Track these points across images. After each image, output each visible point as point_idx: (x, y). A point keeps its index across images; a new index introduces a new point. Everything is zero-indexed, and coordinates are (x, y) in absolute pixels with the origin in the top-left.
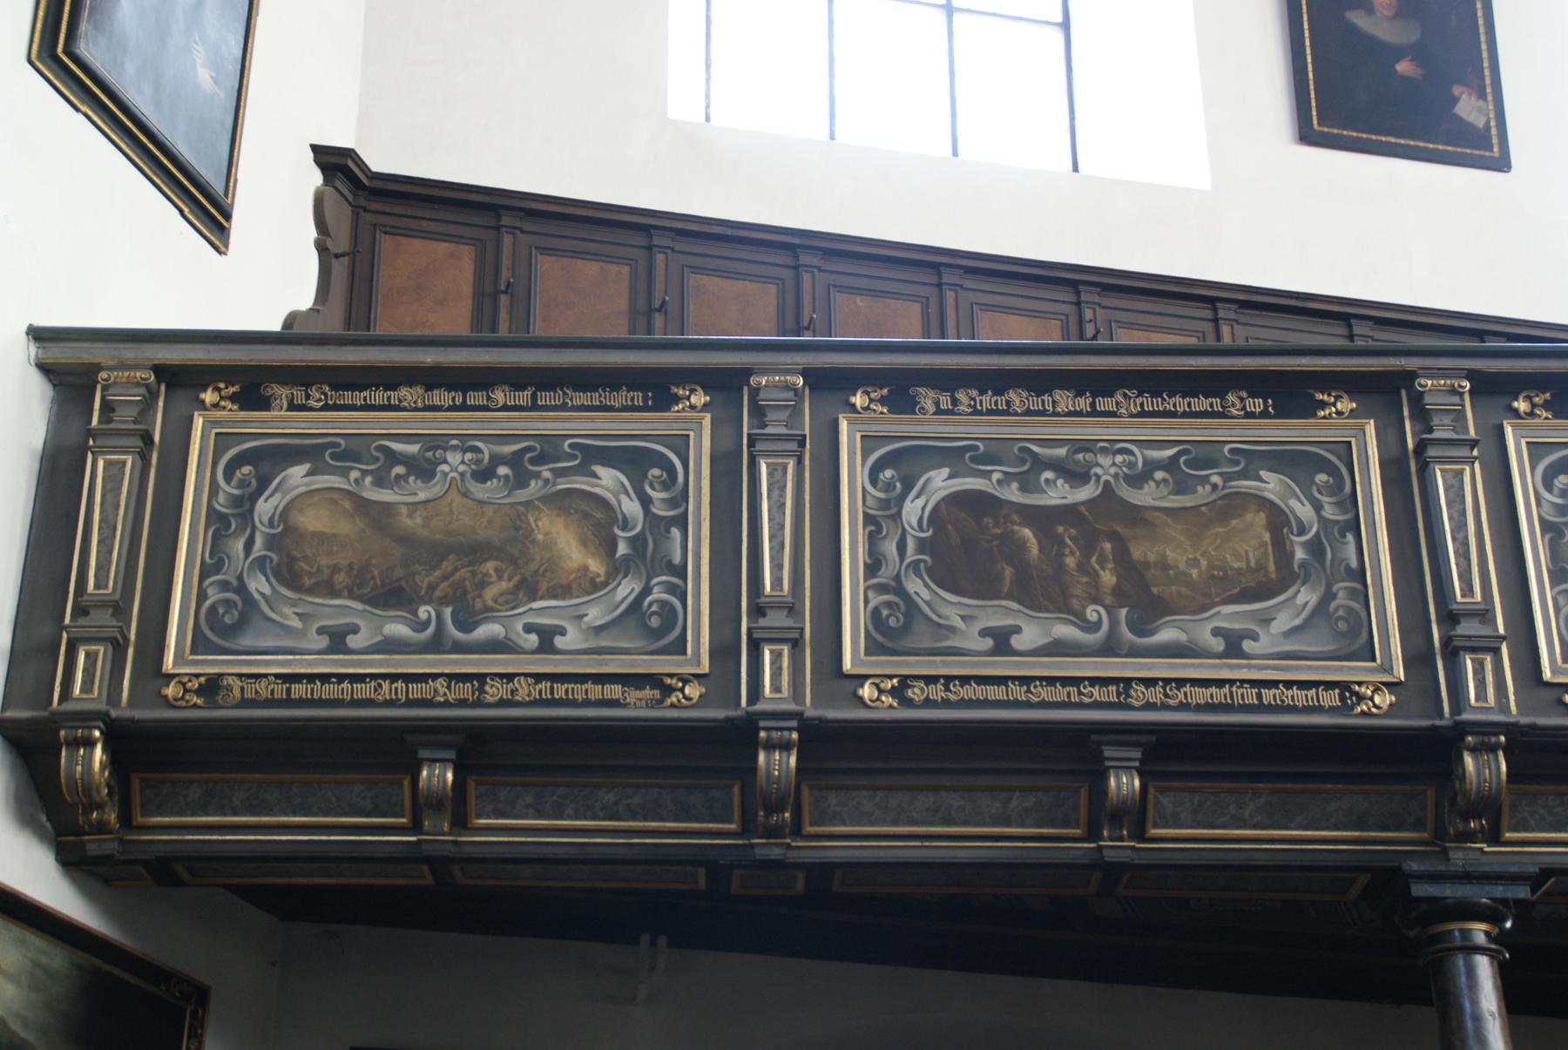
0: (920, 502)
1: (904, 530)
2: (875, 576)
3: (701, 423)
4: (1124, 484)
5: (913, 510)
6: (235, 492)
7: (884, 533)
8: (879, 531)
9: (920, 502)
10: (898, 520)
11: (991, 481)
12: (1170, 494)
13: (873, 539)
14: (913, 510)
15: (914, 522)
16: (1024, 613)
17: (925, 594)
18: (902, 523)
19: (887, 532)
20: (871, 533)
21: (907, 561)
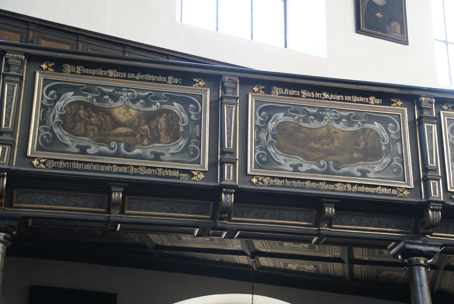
0: (274, 123)
1: (268, 131)
2: (258, 145)
3: (206, 91)
4: (334, 122)
5: (271, 125)
6: (50, 99)
7: (261, 132)
8: (260, 131)
9: (274, 123)
10: (267, 129)
11: (294, 118)
12: (346, 127)
13: (258, 134)
14: (271, 125)
15: (271, 129)
16: (299, 159)
17: (273, 151)
18: (268, 129)
19: (263, 131)
20: (257, 131)
21: (268, 141)
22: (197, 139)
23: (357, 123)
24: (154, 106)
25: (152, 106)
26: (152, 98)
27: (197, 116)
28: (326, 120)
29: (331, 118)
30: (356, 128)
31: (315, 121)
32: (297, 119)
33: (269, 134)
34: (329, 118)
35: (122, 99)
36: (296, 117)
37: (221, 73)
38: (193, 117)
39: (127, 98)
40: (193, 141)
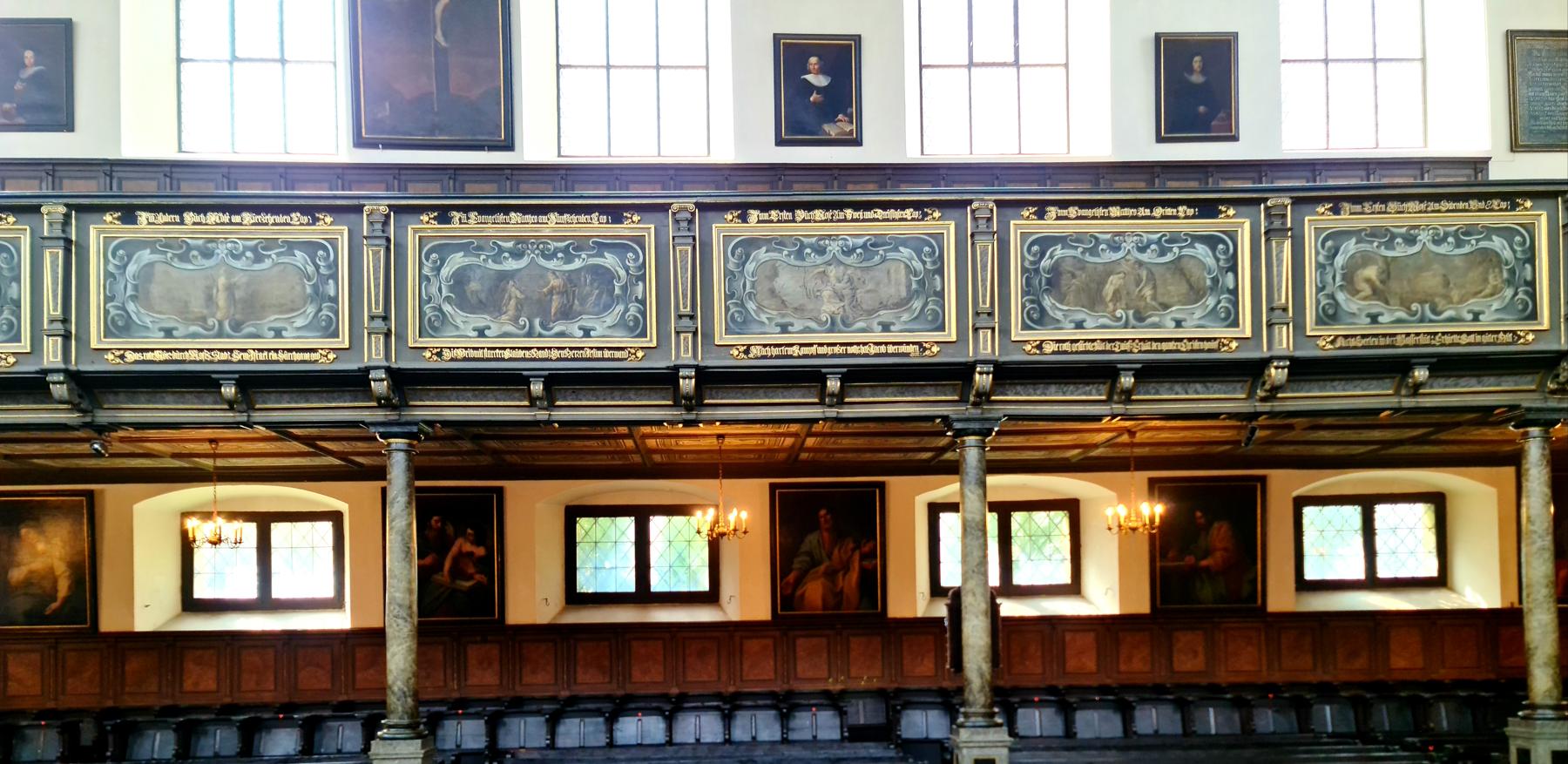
22: (331, 302)
23: (579, 256)
24: (266, 260)
25: (264, 261)
26: (263, 249)
27: (329, 267)
28: (529, 255)
29: (537, 252)
30: (577, 264)
31: (510, 259)
32: (484, 260)
33: (442, 285)
34: (534, 253)
35: (218, 254)
36: (482, 257)
37: (362, 202)
38: (323, 271)
39: (226, 251)
40: (327, 307)
